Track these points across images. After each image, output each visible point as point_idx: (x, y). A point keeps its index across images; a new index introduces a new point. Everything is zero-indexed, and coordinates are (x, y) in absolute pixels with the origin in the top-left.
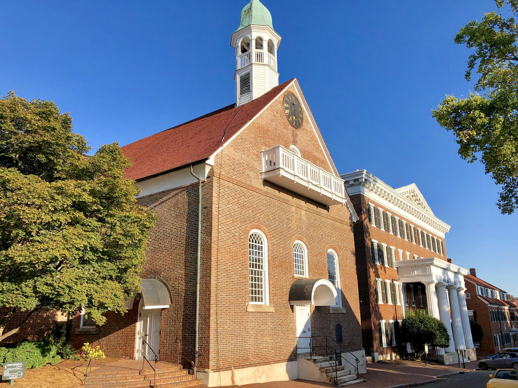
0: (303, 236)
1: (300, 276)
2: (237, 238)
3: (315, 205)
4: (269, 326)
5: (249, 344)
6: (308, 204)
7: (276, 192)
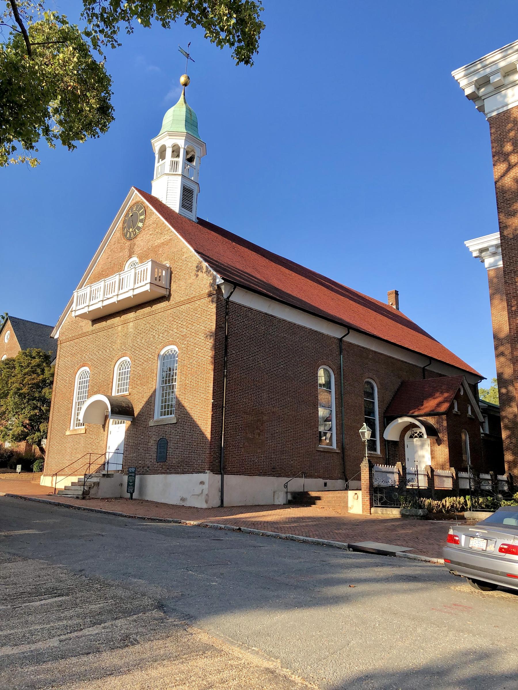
0: (126, 352)
1: (122, 393)
2: (67, 381)
3: (148, 307)
4: (81, 445)
5: (66, 459)
6: (139, 311)
7: (104, 324)
